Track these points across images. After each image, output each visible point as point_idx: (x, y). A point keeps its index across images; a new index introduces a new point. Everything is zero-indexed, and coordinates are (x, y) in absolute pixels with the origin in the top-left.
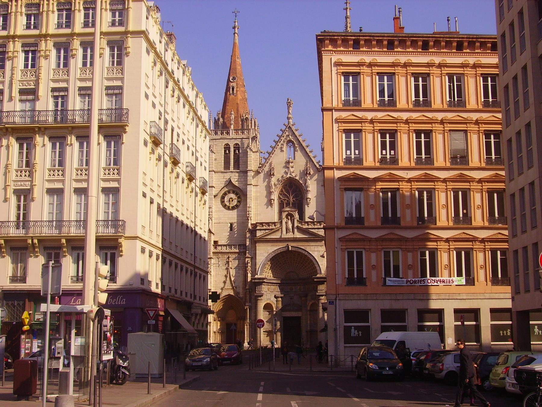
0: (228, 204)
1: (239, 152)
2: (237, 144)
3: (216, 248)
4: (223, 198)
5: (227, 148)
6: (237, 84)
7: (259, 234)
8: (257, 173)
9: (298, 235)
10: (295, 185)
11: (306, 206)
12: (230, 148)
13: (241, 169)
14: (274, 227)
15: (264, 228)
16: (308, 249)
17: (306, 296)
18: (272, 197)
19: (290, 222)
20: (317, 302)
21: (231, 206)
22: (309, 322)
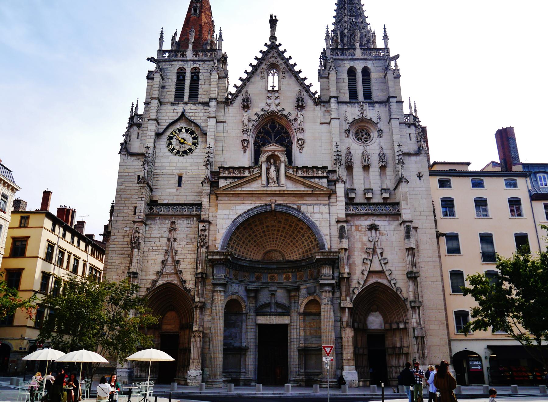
0: (177, 148)
1: (198, 77)
2: (195, 68)
3: (151, 209)
4: (170, 138)
5: (181, 73)
7: (222, 183)
10: (279, 125)
12: (185, 73)
13: (200, 100)
15: (231, 175)
16: (304, 208)
17: (298, 289)
20: (318, 298)
21: (182, 149)
22: (302, 333)
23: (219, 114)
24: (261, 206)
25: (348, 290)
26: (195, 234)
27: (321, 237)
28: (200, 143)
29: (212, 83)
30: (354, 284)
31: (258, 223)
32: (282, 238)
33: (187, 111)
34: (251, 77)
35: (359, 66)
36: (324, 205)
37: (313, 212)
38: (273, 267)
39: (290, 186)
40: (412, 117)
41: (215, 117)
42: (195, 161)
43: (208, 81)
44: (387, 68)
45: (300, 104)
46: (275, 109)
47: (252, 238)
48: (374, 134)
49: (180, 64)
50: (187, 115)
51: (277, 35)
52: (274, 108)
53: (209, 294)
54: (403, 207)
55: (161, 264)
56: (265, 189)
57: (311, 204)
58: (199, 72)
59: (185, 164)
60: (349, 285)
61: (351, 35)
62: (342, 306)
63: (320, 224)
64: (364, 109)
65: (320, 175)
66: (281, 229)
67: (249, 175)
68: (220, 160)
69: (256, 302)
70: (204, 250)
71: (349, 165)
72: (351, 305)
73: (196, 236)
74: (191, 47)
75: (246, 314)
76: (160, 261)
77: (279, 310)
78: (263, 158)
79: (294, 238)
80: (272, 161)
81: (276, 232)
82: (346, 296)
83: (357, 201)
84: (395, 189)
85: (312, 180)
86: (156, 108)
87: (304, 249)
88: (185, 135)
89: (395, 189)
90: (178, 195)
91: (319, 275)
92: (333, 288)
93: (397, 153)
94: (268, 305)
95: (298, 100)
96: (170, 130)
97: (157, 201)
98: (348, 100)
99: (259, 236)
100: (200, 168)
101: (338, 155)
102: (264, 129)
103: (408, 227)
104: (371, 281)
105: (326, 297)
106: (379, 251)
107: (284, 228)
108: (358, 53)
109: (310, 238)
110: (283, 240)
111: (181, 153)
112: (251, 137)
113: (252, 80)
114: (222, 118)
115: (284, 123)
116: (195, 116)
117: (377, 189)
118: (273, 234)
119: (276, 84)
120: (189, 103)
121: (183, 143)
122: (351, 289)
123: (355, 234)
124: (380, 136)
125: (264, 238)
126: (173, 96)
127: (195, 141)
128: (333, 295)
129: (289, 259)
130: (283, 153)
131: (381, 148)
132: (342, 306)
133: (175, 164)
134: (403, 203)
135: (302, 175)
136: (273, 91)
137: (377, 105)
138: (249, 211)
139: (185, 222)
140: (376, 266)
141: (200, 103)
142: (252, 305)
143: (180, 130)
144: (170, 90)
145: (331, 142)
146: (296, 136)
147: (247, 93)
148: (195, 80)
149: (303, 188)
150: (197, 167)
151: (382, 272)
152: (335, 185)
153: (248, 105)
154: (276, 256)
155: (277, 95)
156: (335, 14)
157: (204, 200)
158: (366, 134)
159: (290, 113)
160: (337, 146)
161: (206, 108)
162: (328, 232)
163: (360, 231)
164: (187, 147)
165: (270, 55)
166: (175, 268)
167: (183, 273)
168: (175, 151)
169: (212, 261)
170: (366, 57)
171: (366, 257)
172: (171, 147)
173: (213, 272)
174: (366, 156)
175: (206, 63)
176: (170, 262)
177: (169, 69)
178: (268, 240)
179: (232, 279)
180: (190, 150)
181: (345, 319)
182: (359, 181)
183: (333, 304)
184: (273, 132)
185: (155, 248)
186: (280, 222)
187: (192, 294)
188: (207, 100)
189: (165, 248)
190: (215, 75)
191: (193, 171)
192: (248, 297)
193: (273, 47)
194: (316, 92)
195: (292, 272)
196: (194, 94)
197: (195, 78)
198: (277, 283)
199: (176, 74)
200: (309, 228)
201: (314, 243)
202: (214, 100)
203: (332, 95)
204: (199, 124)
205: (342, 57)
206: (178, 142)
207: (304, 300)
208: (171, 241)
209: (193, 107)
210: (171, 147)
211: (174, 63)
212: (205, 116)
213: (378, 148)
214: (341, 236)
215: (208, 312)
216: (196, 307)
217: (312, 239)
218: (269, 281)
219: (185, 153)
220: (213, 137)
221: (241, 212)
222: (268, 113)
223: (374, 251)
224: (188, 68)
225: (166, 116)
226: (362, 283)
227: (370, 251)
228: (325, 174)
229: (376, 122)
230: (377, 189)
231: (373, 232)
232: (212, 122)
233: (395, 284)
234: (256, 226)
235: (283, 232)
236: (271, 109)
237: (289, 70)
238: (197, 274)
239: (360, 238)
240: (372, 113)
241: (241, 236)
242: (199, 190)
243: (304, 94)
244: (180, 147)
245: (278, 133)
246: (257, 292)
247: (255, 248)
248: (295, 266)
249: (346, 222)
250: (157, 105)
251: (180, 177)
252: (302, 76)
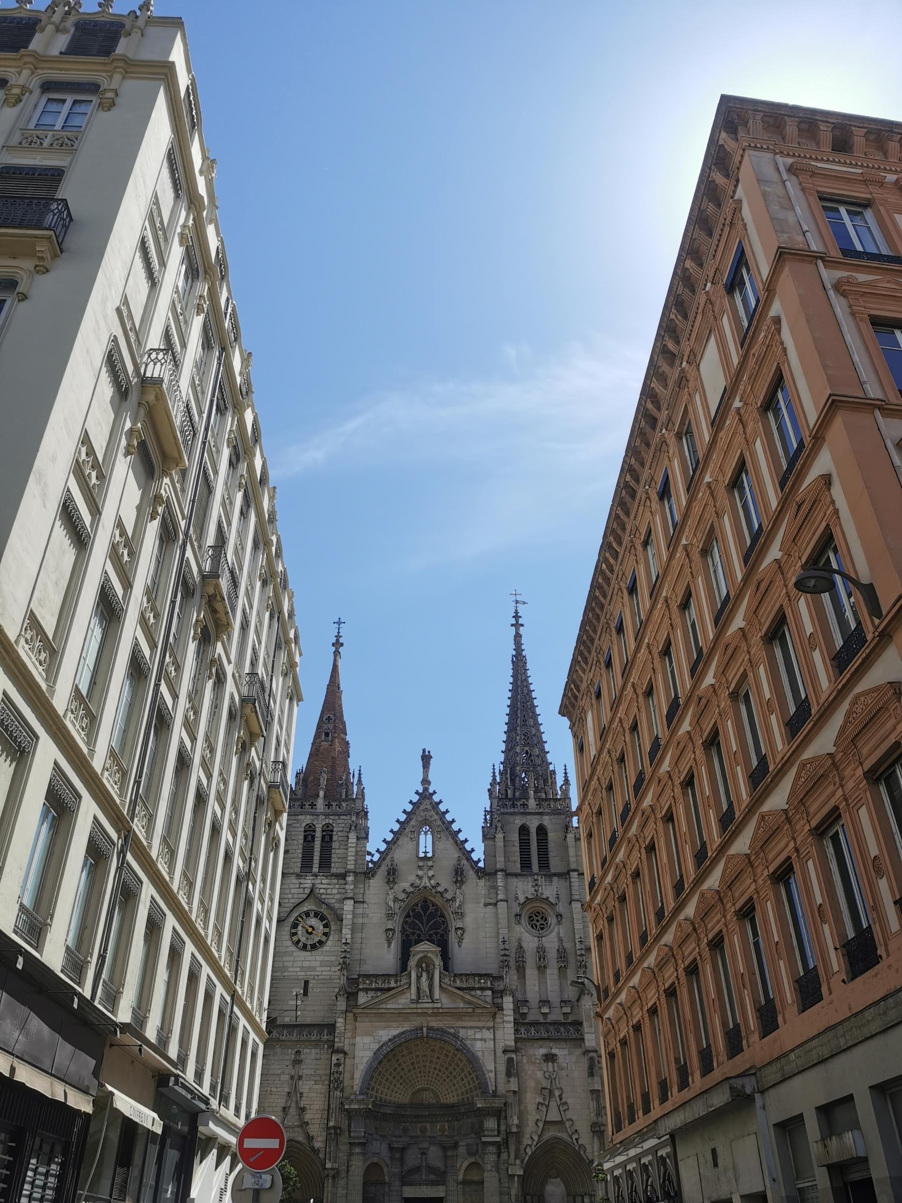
0: (303, 939)
1: (331, 836)
2: (328, 825)
4: (295, 926)
7: (362, 998)
10: (433, 905)
12: (314, 831)
13: (334, 870)
14: (393, 984)
15: (374, 986)
16: (462, 1033)
17: (456, 1146)
19: (424, 975)
20: (480, 1161)
21: (310, 942)
23: (357, 891)
24: (410, 1031)
25: (517, 1150)
26: (326, 1069)
27: (484, 1074)
29: (350, 849)
30: (526, 1141)
31: (405, 1052)
32: (436, 1072)
33: (317, 886)
34: (398, 839)
35: (533, 823)
36: (488, 1029)
37: (475, 1039)
38: (423, 1113)
39: (446, 1002)
42: (326, 958)
43: (343, 843)
44: (567, 827)
46: (428, 884)
47: (398, 1074)
48: (552, 920)
49: (307, 820)
51: (430, 778)
52: (425, 881)
53: (343, 1156)
54: (586, 1031)
55: (281, 1113)
56: (415, 1006)
57: (471, 1028)
58: (332, 831)
59: (313, 964)
60: (519, 1142)
62: (510, 1173)
63: (483, 1056)
65: (483, 985)
66: (435, 1060)
68: (358, 957)
69: (402, 1165)
70: (338, 1094)
72: (521, 1172)
73: (328, 1072)
74: (322, 793)
75: (390, 1184)
76: (280, 1109)
77: (432, 1177)
78: (412, 962)
79: (451, 1073)
80: (424, 965)
81: (428, 1064)
82: (516, 1158)
83: (530, 1018)
84: (578, 1000)
85: (473, 993)
87: (463, 1090)
88: (313, 921)
89: (578, 1000)
91: (479, 1131)
92: (499, 1149)
93: (579, 952)
94: (417, 1169)
95: (457, 873)
96: (295, 914)
98: (519, 871)
99: (406, 1069)
100: (333, 969)
101: (505, 955)
102: (413, 910)
103: (592, 1059)
104: (548, 1135)
105: (491, 1158)
106: (557, 1093)
107: (438, 1058)
109: (470, 1074)
110: (438, 1075)
111: (309, 947)
112: (396, 924)
113: (400, 842)
114: (361, 896)
115: (438, 901)
116: (327, 894)
117: (554, 998)
118: (425, 1066)
119: (429, 849)
121: (311, 933)
122: (522, 1147)
123: (527, 1067)
124: (559, 923)
125: (413, 1072)
127: (327, 930)
128: (499, 1156)
129: (445, 1101)
131: (560, 940)
132: (510, 1173)
133: (300, 964)
134: (585, 1024)
136: (426, 858)
137: (555, 879)
138: (395, 1037)
139: (313, 1051)
140: (554, 1116)
141: (333, 875)
142: (396, 1170)
145: (498, 934)
146: (455, 923)
147: (392, 860)
149: (462, 1005)
150: (328, 968)
151: (561, 1122)
152: (502, 997)
154: (428, 1098)
155: (430, 863)
156: (504, 737)
157: (339, 1020)
160: (504, 942)
161: (341, 881)
162: (491, 1067)
163: (534, 1063)
164: (317, 940)
165: (422, 807)
166: (300, 1119)
167: (310, 1126)
168: (301, 944)
169: (348, 1111)
170: (541, 810)
171: (542, 1101)
172: (295, 938)
173: (349, 1126)
174: (541, 953)
175: (342, 817)
176: (293, 1111)
178: (419, 1075)
179: (372, 1135)
180: (321, 943)
181: (513, 1192)
182: (532, 989)
183: (498, 1172)
184: (425, 921)
185: (274, 1090)
186: (433, 1050)
187: (321, 1156)
188: (342, 871)
189: (287, 1090)
190: (353, 837)
192: (392, 1159)
193: (425, 795)
194: (479, 860)
195: (448, 1121)
196: (325, 863)
198: (429, 1137)
200: (470, 1062)
201: (477, 1082)
203: (498, 866)
205: (512, 810)
206: (304, 931)
207: (463, 1162)
208: (296, 1079)
210: (295, 938)
211: (300, 817)
212: (339, 893)
213: (556, 940)
214: (509, 1074)
215: (342, 1182)
216: (328, 1176)
217: (473, 1075)
218: (419, 1133)
219: (314, 947)
221: (385, 1039)
223: (551, 1092)
225: (290, 893)
226: (536, 1138)
227: (546, 1092)
230: (554, 998)
231: (550, 1064)
232: (348, 906)
233: (577, 1140)
234: (403, 1056)
235: (436, 1063)
236: (423, 884)
237: (445, 829)
238: (328, 1128)
239: (534, 1073)
240: (549, 890)
241: (384, 1072)
242: (330, 1002)
243: (464, 862)
245: (432, 916)
246: (403, 1150)
247: (401, 1087)
248: (451, 1112)
249: (516, 1050)
251: (306, 983)
252: (462, 837)
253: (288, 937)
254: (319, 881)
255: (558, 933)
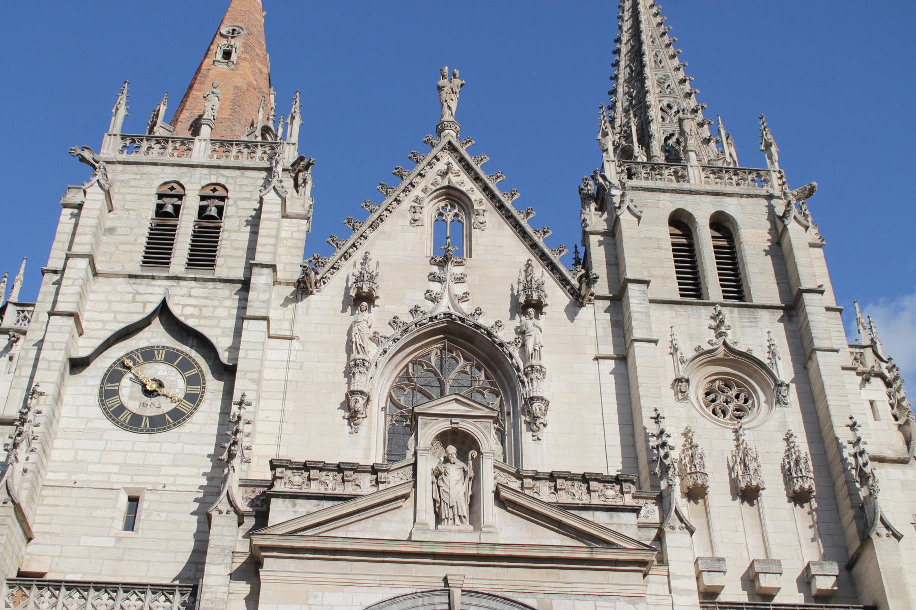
1: (220, 210)
2: (215, 186)
6: (247, 46)
7: (279, 512)
8: (303, 288)
9: (506, 530)
11: (526, 436)
12: (180, 197)
15: (315, 488)
18: (360, 382)
19: (454, 472)
28: (207, 395)
35: (702, 212)
40: (868, 352)
41: (266, 319)
42: (188, 449)
45: (535, 297)
50: (176, 310)
61: (667, 139)
64: (727, 323)
65: (610, 502)
67: (374, 489)
71: (695, 485)
74: (205, 131)
86: (80, 282)
90: (121, 560)
95: (527, 287)
97: (42, 575)
108: (696, 177)
111: (146, 423)
114: (286, 325)
116: (201, 317)
120: (184, 279)
124: (781, 401)
126: (140, 257)
127: (195, 389)
130: (486, 427)
131: (788, 438)
135: (553, 499)
143: (148, 355)
144: (131, 239)
148: (212, 217)
153: (371, 290)
155: (458, 270)
158: (737, 397)
159: (499, 324)
164: (166, 406)
165: (441, 166)
168: (125, 417)
170: (718, 188)
172: (112, 403)
177: (132, 183)
191: (179, 481)
196: (204, 252)
197: (213, 212)
199: (154, 201)
202: (266, 271)
204: (214, 340)
205: (650, 184)
209: (198, 289)
210: (112, 403)
219: (158, 424)
220: (256, 376)
222: (431, 319)
224: (194, 185)
228: (628, 500)
229: (766, 362)
244: (144, 405)
250: (83, 274)
251: (134, 500)
253: (95, 399)
254: (184, 291)
255: (784, 423)
